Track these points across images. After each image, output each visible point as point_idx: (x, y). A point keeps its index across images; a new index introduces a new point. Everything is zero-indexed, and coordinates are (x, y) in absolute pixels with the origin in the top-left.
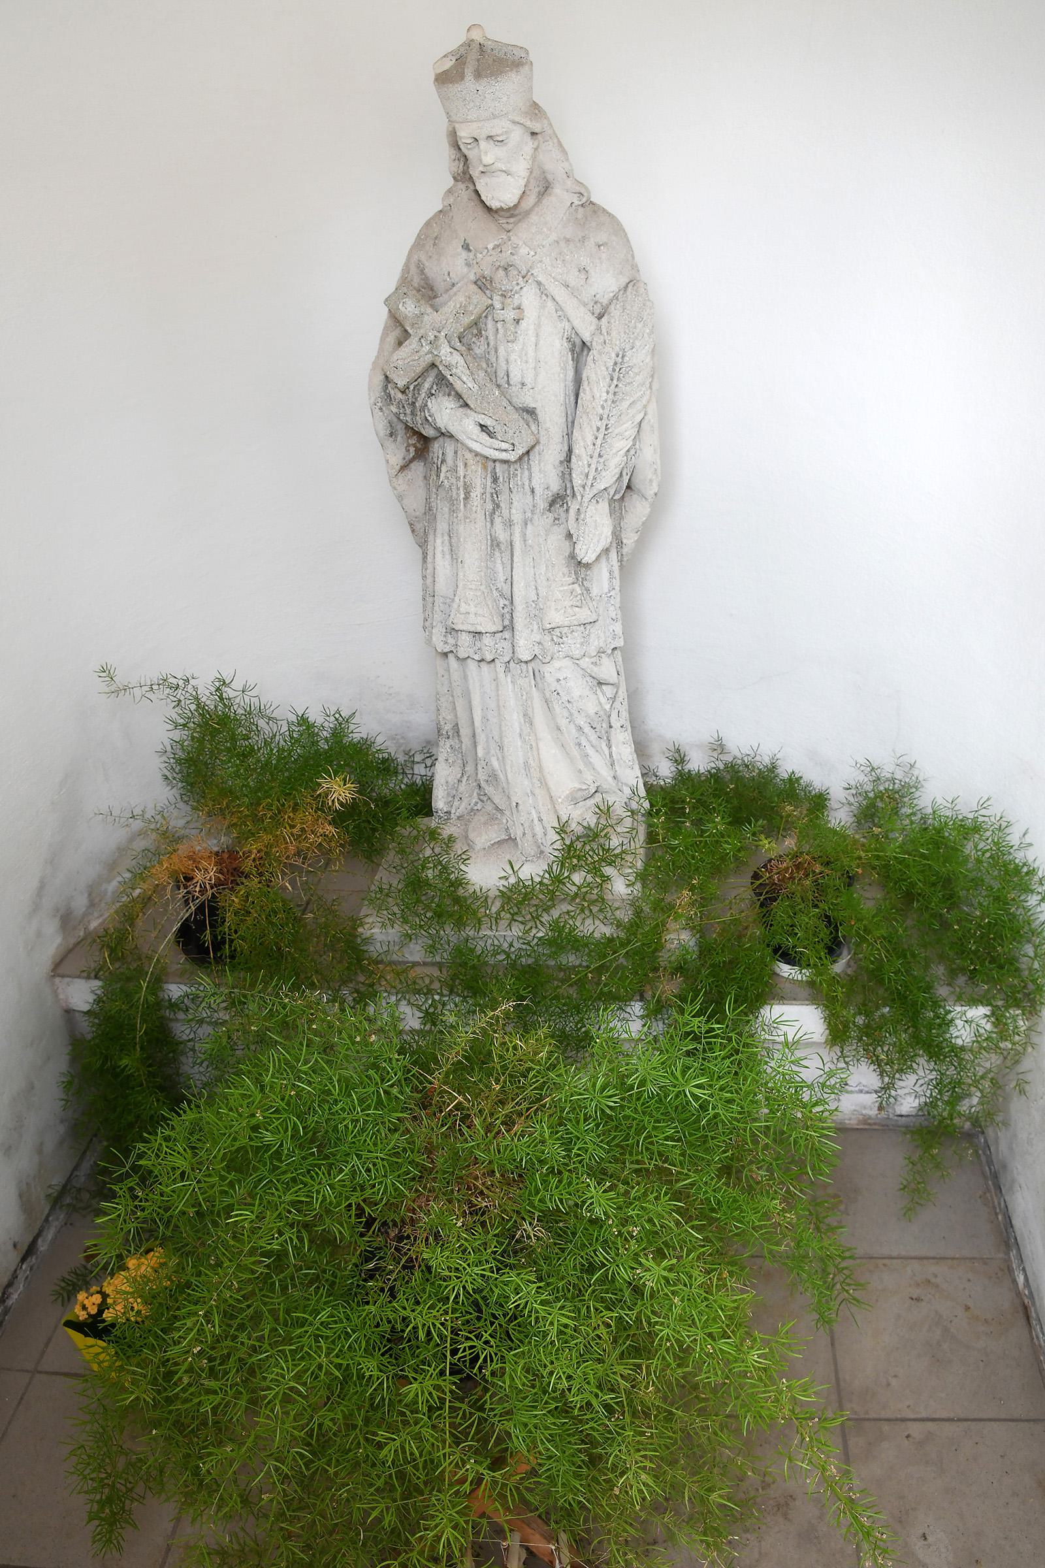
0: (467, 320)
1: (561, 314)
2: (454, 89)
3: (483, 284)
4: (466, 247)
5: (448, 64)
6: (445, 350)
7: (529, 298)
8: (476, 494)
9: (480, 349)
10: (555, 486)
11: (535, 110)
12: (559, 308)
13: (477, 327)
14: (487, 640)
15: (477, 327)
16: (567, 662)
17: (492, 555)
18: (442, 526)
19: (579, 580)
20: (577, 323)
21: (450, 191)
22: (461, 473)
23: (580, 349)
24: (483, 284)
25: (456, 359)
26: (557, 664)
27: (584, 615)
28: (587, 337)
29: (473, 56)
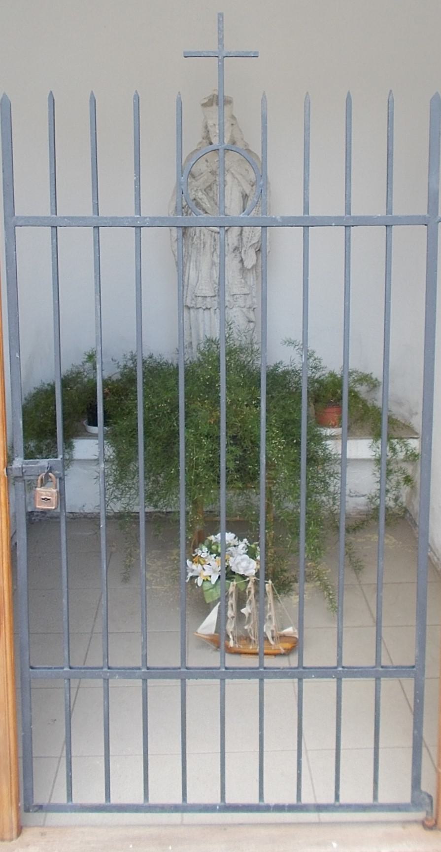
0: (208, 184)
1: (240, 185)
2: (209, 109)
3: (213, 173)
4: (207, 161)
5: (206, 101)
6: (200, 193)
7: (228, 178)
8: (207, 246)
9: (211, 195)
10: (236, 244)
11: (233, 117)
12: (239, 182)
13: (210, 187)
14: (208, 299)
15: (210, 187)
16: (238, 309)
17: (211, 268)
18: (193, 258)
19: (244, 278)
20: (244, 187)
21: (200, 143)
22: (202, 237)
23: (245, 197)
24: (213, 173)
25: (204, 196)
26: (234, 309)
27: (246, 291)
28: (248, 192)
29: (215, 99)
